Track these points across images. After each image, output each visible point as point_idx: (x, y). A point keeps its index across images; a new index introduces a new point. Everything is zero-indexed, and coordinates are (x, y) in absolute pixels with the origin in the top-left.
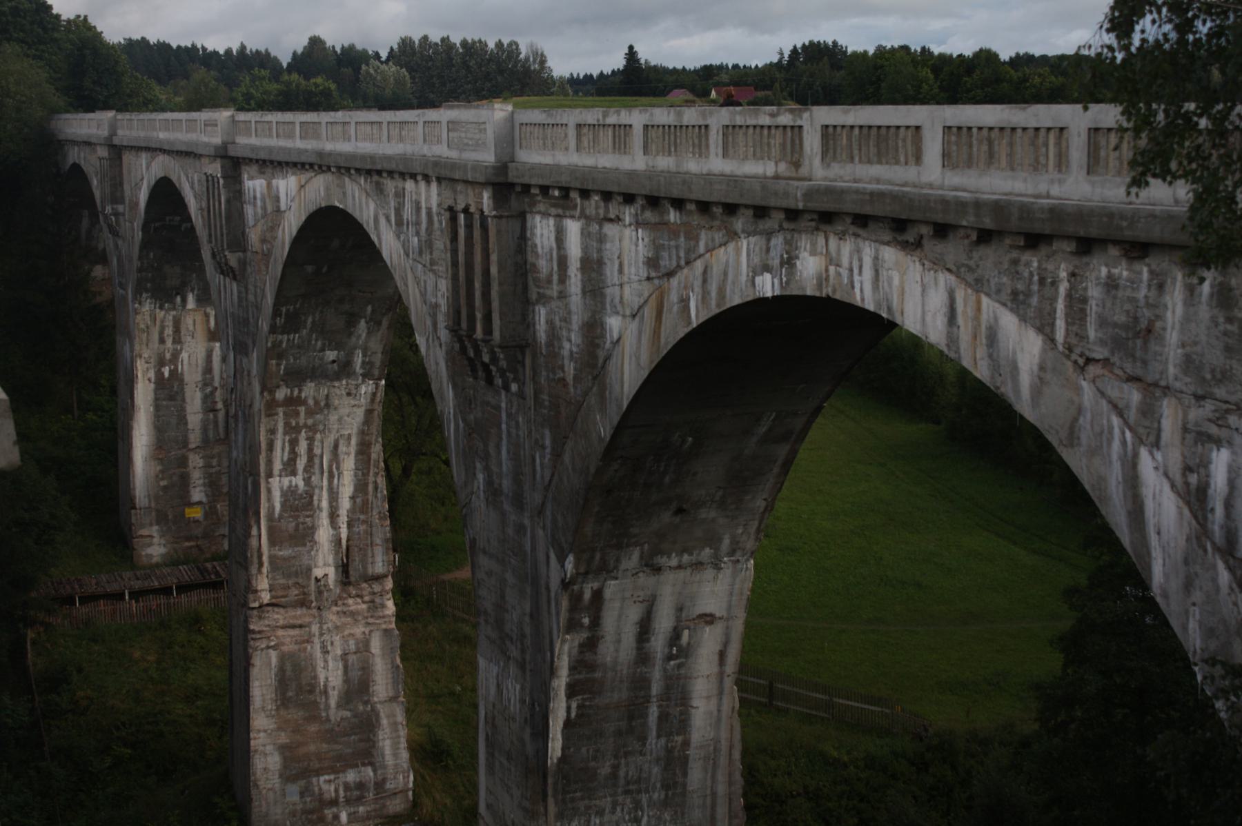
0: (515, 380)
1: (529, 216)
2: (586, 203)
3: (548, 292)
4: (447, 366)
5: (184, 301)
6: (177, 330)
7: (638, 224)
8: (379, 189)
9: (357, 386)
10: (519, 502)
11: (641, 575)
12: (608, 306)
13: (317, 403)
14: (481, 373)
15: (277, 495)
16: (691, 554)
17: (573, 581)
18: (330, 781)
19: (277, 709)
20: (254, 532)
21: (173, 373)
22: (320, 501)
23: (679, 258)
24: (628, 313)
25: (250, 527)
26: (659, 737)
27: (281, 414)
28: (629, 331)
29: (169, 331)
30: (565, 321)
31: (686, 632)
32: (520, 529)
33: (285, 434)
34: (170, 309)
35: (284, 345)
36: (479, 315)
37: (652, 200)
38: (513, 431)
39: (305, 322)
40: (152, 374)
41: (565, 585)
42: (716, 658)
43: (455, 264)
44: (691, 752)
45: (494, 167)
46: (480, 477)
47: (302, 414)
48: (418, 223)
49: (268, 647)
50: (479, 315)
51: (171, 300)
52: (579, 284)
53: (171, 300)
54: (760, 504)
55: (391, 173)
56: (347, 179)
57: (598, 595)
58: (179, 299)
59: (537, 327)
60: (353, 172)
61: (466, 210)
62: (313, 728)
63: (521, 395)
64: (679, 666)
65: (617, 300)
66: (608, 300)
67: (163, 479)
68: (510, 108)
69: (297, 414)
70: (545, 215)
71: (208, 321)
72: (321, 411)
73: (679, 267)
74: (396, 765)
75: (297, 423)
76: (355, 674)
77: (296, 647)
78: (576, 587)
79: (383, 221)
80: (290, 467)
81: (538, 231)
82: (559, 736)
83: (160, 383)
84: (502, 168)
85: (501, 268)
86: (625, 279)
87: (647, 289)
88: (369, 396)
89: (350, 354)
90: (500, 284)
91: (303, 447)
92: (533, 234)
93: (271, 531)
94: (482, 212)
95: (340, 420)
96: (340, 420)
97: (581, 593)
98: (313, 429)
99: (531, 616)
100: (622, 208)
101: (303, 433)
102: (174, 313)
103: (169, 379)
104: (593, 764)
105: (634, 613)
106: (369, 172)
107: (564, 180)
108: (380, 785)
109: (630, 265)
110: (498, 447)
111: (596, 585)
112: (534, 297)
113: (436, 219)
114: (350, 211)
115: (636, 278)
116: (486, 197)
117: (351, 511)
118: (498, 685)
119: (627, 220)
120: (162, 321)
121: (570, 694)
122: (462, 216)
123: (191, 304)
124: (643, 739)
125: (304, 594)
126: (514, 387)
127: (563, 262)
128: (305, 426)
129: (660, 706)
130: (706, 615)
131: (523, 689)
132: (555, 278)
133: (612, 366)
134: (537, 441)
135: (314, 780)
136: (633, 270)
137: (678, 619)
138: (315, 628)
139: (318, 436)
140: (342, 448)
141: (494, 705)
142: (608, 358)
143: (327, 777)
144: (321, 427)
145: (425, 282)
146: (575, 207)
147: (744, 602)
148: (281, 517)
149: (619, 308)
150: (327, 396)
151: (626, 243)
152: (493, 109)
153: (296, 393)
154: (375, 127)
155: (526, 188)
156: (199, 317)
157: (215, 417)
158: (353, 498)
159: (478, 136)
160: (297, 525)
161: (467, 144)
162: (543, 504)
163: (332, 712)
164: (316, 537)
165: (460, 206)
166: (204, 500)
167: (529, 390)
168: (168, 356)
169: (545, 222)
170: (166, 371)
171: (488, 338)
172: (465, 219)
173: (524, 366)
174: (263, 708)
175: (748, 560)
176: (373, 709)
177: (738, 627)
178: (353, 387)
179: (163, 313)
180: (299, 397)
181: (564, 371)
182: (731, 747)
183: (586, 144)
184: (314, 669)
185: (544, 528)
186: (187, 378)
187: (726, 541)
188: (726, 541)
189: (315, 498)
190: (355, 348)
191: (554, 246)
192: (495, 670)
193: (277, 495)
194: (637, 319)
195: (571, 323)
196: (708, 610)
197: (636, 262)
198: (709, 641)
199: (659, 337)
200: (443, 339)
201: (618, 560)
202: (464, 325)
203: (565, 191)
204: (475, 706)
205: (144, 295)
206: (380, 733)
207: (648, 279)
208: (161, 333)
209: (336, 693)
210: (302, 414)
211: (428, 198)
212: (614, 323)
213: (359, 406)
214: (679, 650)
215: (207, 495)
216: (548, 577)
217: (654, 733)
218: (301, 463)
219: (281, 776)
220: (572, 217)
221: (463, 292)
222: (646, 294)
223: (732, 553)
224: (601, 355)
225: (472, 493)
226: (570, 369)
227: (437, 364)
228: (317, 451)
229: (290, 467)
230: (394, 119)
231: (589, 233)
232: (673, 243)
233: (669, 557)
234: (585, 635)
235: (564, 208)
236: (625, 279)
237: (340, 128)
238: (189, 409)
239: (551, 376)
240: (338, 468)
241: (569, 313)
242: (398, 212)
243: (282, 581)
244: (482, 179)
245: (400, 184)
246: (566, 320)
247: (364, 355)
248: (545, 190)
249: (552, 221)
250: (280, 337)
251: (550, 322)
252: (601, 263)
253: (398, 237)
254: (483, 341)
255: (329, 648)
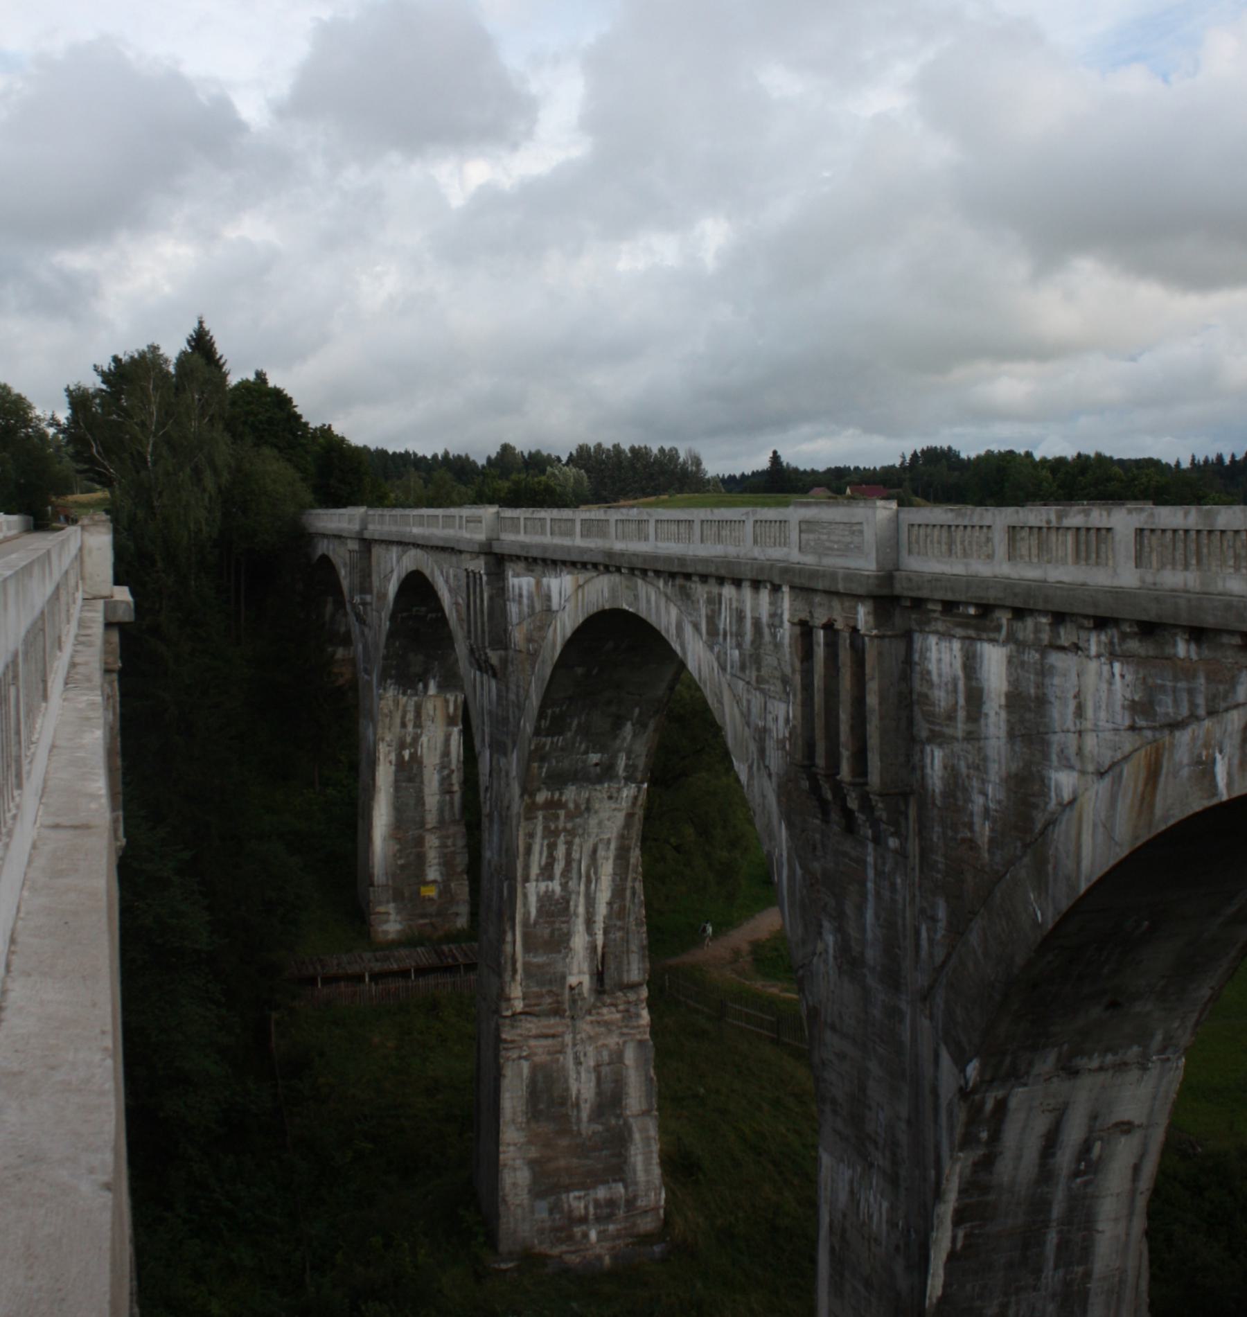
0: (896, 834)
1: (918, 638)
2: (1018, 625)
3: (948, 731)
4: (779, 802)
5: (426, 687)
6: (418, 714)
7: (1113, 656)
8: (686, 595)
9: (619, 790)
10: (892, 978)
11: (1055, 1080)
12: (1054, 757)
13: (577, 806)
14: (835, 816)
15: (533, 900)
16: (1115, 1053)
17: (975, 1090)
18: (579, 1198)
19: (528, 1122)
20: (509, 938)
21: (413, 756)
22: (576, 906)
23: (1193, 705)
24: (1090, 768)
25: (504, 932)
26: (1056, 1268)
27: (540, 818)
28: (1091, 793)
29: (410, 716)
30: (977, 768)
31: (1098, 1145)
32: (894, 1013)
33: (543, 838)
34: (412, 695)
35: (547, 747)
36: (845, 754)
37: (1141, 629)
38: (886, 894)
39: (571, 724)
40: (393, 757)
41: (964, 1093)
42: (1129, 1172)
43: (807, 687)
44: (1092, 1285)
45: (877, 577)
46: (830, 939)
47: (562, 818)
48: (739, 634)
49: (520, 1058)
50: (845, 754)
52: (1003, 727)
54: (1206, 992)
55: (704, 578)
56: (640, 582)
57: (1001, 1106)
58: (421, 685)
59: (929, 771)
60: (651, 574)
61: (829, 627)
62: (564, 1142)
63: (902, 853)
64: (1086, 1184)
65: (1072, 750)
66: (1055, 749)
67: (400, 858)
68: (894, 505)
69: (557, 818)
70: (946, 636)
71: (447, 707)
72: (580, 815)
73: (1194, 717)
74: (648, 1182)
75: (557, 827)
76: (608, 1087)
77: (548, 1058)
78: (977, 1097)
79: (689, 630)
80: (547, 872)
81: (933, 655)
82: (941, 1272)
83: (401, 765)
84: (888, 577)
85: (882, 699)
86: (1089, 725)
87: (1128, 742)
88: (630, 800)
89: (614, 757)
90: (881, 718)
91: (561, 852)
92: (924, 658)
93: (526, 936)
94: (855, 630)
95: (600, 824)
96: (600, 824)
97: (983, 1103)
98: (572, 833)
99: (909, 1122)
100: (1083, 634)
101: (562, 838)
102: (415, 698)
103: (409, 762)
104: (978, 1303)
105: (1041, 1124)
106: (672, 575)
107: (992, 596)
108: (630, 1203)
109: (1097, 708)
110: (860, 909)
111: (1000, 1094)
112: (924, 734)
113: (766, 631)
114: (643, 615)
115: (1110, 726)
116: (863, 615)
117: (608, 918)
118: (852, 1192)
119: (1093, 650)
120: (405, 706)
121: (957, 1223)
122: (821, 632)
123: (432, 690)
124: (1037, 1271)
125: (558, 1002)
126: (893, 843)
127: (975, 697)
128: (565, 830)
129: (1060, 1232)
130: (1123, 1123)
131: (893, 1208)
132: (961, 714)
133: (1059, 834)
134: (922, 911)
135: (564, 1196)
136: (1103, 715)
137: (1091, 1130)
138: (568, 1038)
139: (577, 840)
140: (601, 853)
141: (844, 1216)
142: (1052, 822)
143: (577, 1194)
144: (580, 831)
145: (749, 701)
146: (998, 628)
147: (1169, 1106)
148: (536, 923)
149: (1074, 761)
150: (588, 800)
151: (1091, 680)
152: (875, 508)
153: (557, 795)
154: (683, 527)
155: (918, 603)
156: (439, 703)
157: (452, 799)
158: (610, 904)
159: (848, 539)
160: (553, 932)
161: (831, 549)
162: (931, 987)
163: (584, 1125)
164: (572, 945)
165: (820, 618)
166: (439, 878)
167: (914, 847)
168: (409, 740)
169: (944, 644)
170: (406, 754)
171: (861, 780)
172: (825, 636)
173: (907, 818)
174: (513, 1121)
175: (1179, 1058)
176: (626, 1123)
177: (1158, 1135)
178: (614, 791)
179: (405, 698)
180: (560, 800)
181: (971, 829)
182: (1138, 1277)
183: (1024, 551)
184: (566, 1081)
185: (931, 1017)
186: (426, 761)
187: (1159, 1037)
188: (1159, 1037)
189: (572, 903)
190: (619, 751)
191: (960, 673)
192: (848, 1174)
193: (533, 900)
194: (1107, 780)
195: (986, 772)
196: (1126, 1118)
197: (1110, 705)
198: (1124, 1152)
199: (1152, 806)
200: (773, 769)
201: (1031, 1064)
202: (820, 761)
203: (986, 610)
204: (813, 1205)
205: (389, 681)
206: (633, 1148)
207: (1132, 728)
208: (403, 717)
209: (588, 1106)
210: (562, 818)
211: (755, 607)
212: (1064, 781)
213: (619, 810)
214: (1089, 1163)
215: (441, 874)
216: (936, 1078)
217: (1051, 1264)
218: (559, 868)
219: (530, 1191)
220: (991, 641)
221: (819, 723)
222: (1128, 748)
223: (1163, 1050)
224: (1040, 819)
225: (814, 954)
226: (984, 831)
227: (764, 796)
228: (576, 855)
229: (547, 872)
230: (710, 518)
231: (1023, 664)
232: (1182, 685)
233: (1090, 1058)
234: (981, 1152)
235: (977, 629)
236: (1089, 725)
237: (634, 526)
238: (427, 791)
239: (950, 833)
240: (596, 873)
241: (985, 759)
242: (712, 620)
243: (536, 989)
244: (861, 591)
245: (715, 590)
246: (980, 767)
247: (628, 758)
248: (949, 607)
249: (956, 645)
250: (544, 739)
251: (951, 771)
252: (1042, 702)
253: (711, 648)
254: (853, 784)
255: (582, 1059)
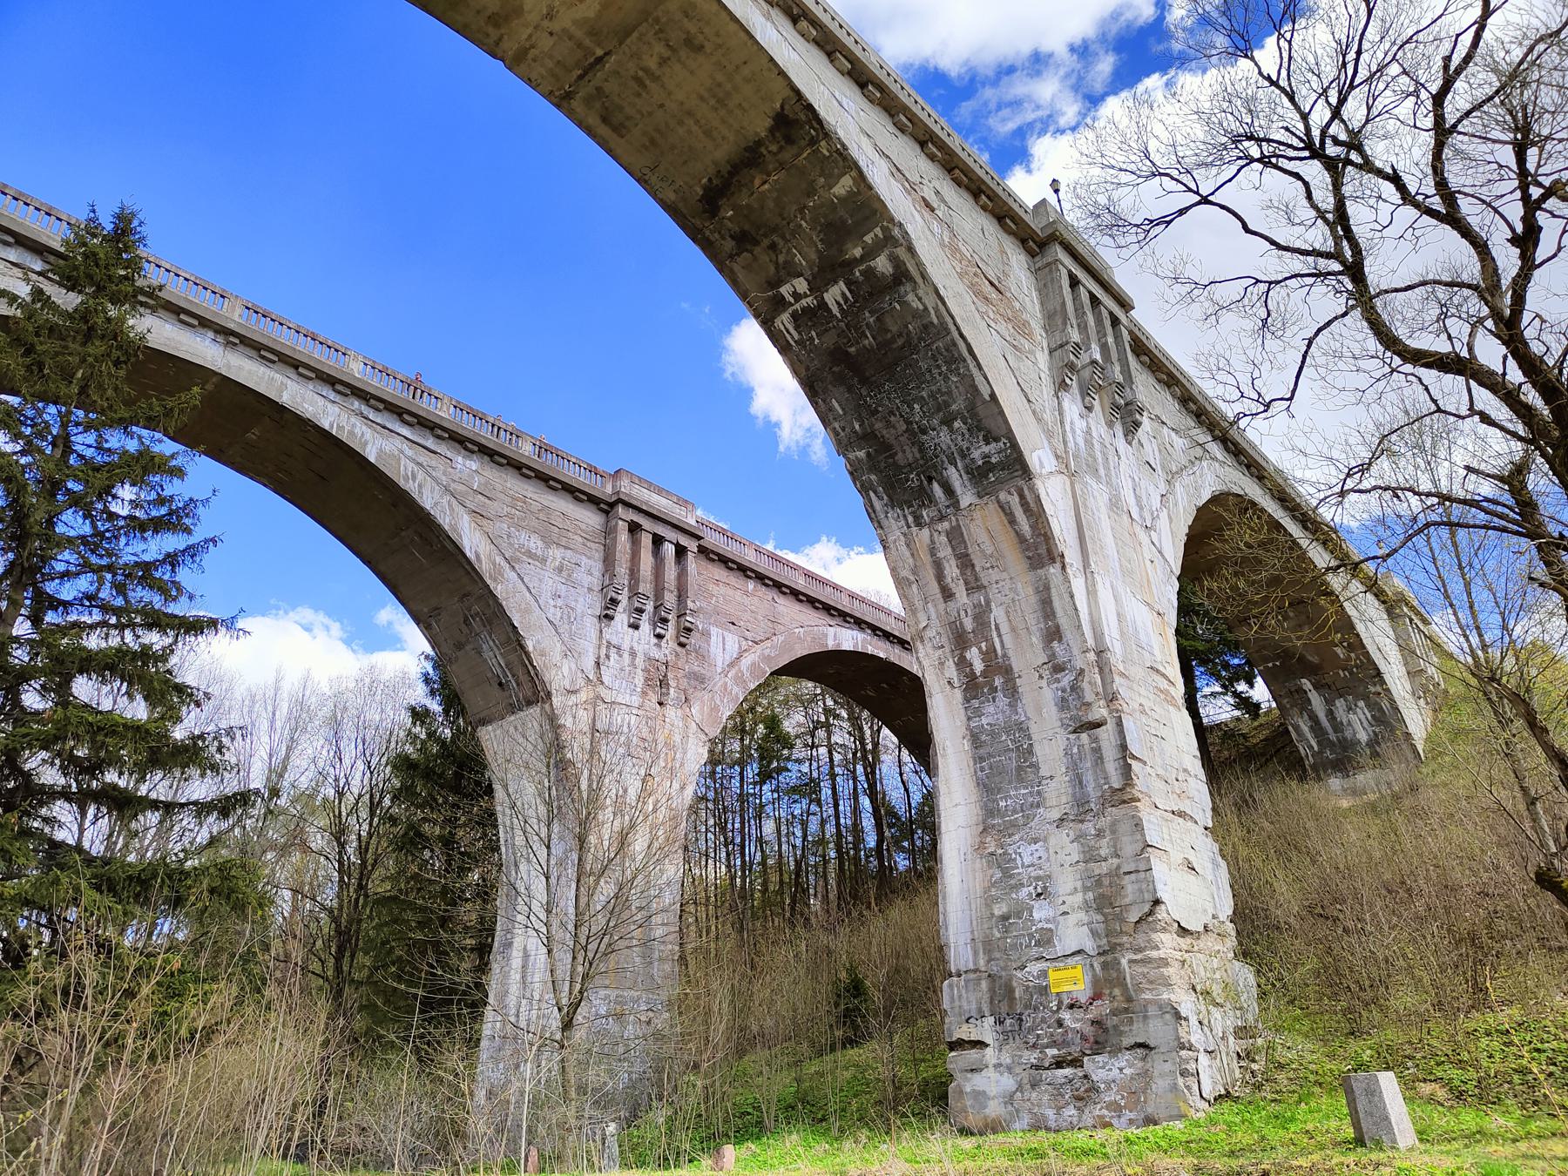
6: (965, 562)
29: (952, 570)
51: (925, 498)
53: (925, 498)
58: (937, 490)
71: (1012, 521)
120: (933, 551)
156: (994, 518)
170: (974, 656)
179: (926, 532)
208: (940, 576)
